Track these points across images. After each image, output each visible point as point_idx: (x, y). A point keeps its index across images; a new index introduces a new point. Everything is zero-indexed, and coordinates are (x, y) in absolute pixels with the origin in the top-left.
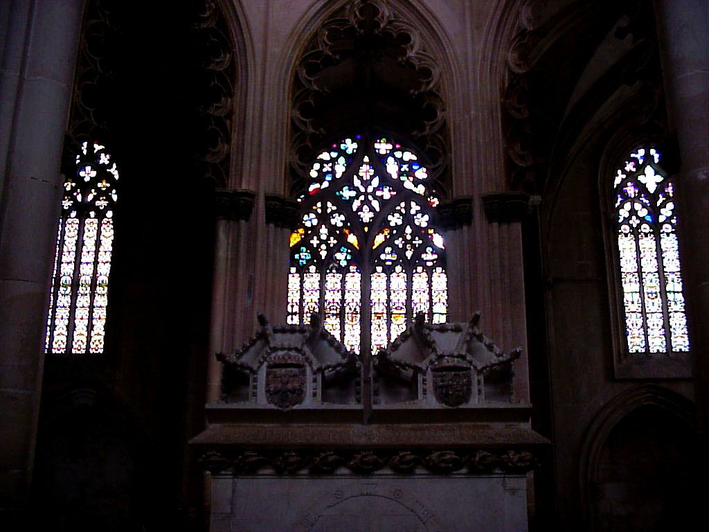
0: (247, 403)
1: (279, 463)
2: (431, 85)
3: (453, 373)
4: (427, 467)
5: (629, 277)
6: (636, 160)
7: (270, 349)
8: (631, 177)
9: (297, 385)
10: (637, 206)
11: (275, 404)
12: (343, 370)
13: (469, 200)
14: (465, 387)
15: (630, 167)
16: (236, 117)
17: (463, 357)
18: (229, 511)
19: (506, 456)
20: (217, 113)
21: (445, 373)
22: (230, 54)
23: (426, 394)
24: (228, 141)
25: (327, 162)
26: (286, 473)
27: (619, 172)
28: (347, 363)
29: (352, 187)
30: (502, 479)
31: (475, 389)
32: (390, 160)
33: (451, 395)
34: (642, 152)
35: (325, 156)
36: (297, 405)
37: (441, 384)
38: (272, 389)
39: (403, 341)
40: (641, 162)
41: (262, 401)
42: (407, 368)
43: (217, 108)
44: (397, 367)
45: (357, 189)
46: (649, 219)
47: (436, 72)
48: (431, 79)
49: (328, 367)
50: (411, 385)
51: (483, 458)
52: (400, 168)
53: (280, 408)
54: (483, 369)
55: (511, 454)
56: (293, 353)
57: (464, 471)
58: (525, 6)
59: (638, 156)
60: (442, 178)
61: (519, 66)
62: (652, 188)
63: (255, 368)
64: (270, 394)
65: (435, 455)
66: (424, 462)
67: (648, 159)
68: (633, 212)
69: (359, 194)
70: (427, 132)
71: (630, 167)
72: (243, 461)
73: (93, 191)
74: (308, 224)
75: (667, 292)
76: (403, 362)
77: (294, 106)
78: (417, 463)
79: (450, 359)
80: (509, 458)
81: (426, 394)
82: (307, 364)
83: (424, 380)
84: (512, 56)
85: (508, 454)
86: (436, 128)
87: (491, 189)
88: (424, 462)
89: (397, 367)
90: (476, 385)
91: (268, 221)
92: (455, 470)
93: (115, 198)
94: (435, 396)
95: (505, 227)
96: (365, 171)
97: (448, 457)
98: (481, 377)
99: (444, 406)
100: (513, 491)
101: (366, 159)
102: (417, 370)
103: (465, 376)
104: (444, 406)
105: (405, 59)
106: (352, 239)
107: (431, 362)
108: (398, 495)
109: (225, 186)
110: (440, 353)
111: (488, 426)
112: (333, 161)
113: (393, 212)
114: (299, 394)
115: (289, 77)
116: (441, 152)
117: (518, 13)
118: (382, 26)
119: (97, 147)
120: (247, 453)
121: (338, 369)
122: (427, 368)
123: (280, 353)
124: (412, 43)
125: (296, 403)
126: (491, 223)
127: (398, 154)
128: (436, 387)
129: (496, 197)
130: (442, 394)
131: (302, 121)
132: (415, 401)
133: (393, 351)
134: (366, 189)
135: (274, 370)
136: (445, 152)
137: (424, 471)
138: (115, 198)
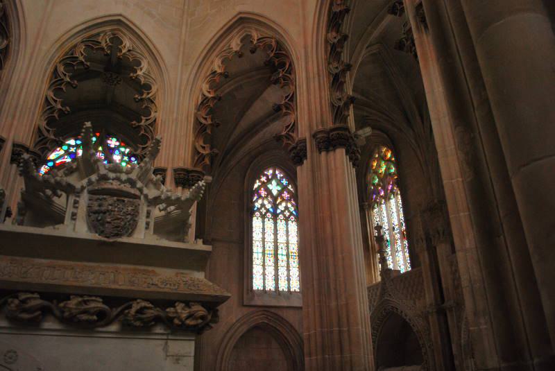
2: (150, 95)
3: (115, 198)
4: (62, 320)
5: (257, 243)
6: (267, 176)
8: (264, 185)
15: (264, 179)
17: (132, 183)
19: (172, 309)
21: (105, 196)
22: (7, 40)
23: (75, 219)
25: (73, 146)
27: (257, 181)
30: (163, 342)
32: (117, 152)
33: (108, 222)
34: (271, 172)
35: (72, 142)
37: (97, 208)
40: (270, 177)
42: (59, 192)
46: (271, 210)
52: (123, 158)
55: (180, 307)
57: (114, 328)
59: (269, 174)
61: (209, 92)
62: (275, 193)
65: (73, 303)
66: (57, 312)
67: (274, 176)
68: (263, 205)
70: (142, 123)
71: (264, 179)
77: (49, 88)
78: (46, 311)
80: (176, 312)
81: (75, 219)
83: (76, 202)
84: (205, 87)
85: (175, 307)
86: (149, 122)
87: (181, 165)
92: (103, 326)
94: (88, 223)
97: (93, 305)
99: (96, 237)
100: (177, 358)
101: (100, 149)
103: (132, 204)
104: (96, 237)
105: (135, 75)
107: (90, 183)
108: (11, 358)
111: (153, 271)
115: (50, 69)
117: (212, 62)
118: (124, 51)
122: (83, 188)
124: (142, 66)
127: (122, 149)
128: (91, 212)
130: (96, 219)
131: (54, 100)
137: (56, 326)
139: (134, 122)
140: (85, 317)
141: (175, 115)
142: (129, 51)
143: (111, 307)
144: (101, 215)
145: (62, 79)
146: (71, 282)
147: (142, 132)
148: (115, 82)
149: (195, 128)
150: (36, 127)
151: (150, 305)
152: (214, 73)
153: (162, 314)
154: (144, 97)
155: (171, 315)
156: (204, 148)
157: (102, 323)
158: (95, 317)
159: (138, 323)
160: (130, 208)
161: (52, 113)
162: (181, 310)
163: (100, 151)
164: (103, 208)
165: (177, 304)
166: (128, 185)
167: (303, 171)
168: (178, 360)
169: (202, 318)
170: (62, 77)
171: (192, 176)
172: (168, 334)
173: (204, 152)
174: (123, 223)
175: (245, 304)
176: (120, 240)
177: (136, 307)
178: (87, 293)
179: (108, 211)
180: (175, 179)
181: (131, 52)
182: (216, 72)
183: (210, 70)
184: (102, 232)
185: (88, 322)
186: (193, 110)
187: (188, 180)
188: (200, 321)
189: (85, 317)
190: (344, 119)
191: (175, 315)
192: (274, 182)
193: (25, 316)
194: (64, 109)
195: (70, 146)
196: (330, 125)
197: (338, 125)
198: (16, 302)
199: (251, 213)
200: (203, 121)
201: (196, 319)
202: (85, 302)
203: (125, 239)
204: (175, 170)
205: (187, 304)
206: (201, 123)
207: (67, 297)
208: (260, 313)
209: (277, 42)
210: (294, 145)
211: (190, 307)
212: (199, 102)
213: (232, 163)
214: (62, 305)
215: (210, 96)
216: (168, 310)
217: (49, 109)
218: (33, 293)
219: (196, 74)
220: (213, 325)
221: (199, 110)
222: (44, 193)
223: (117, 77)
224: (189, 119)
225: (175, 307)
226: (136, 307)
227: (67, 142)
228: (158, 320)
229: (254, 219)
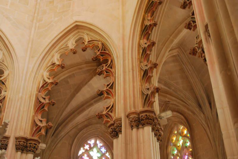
6: (90, 145)
27: (82, 148)
40: (92, 146)
47: (6, 73)
48: (3, 75)
61: (49, 79)
67: (95, 145)
71: (87, 147)
84: (46, 74)
87: (21, 134)
117: (53, 56)
126: (17, 152)
129: (23, 138)
141: (21, 94)
149: (35, 106)
152: (54, 64)
156: (41, 121)
167: (118, 143)
171: (29, 143)
173: (41, 125)
180: (16, 145)
182: (54, 64)
183: (51, 61)
186: (35, 92)
187: (26, 147)
190: (151, 104)
192: (95, 150)
196: (140, 108)
197: (146, 108)
200: (43, 101)
204: (17, 138)
206: (41, 102)
209: (103, 44)
210: (112, 122)
212: (41, 86)
213: (63, 133)
215: (49, 81)
221: (39, 92)
224: (31, 98)
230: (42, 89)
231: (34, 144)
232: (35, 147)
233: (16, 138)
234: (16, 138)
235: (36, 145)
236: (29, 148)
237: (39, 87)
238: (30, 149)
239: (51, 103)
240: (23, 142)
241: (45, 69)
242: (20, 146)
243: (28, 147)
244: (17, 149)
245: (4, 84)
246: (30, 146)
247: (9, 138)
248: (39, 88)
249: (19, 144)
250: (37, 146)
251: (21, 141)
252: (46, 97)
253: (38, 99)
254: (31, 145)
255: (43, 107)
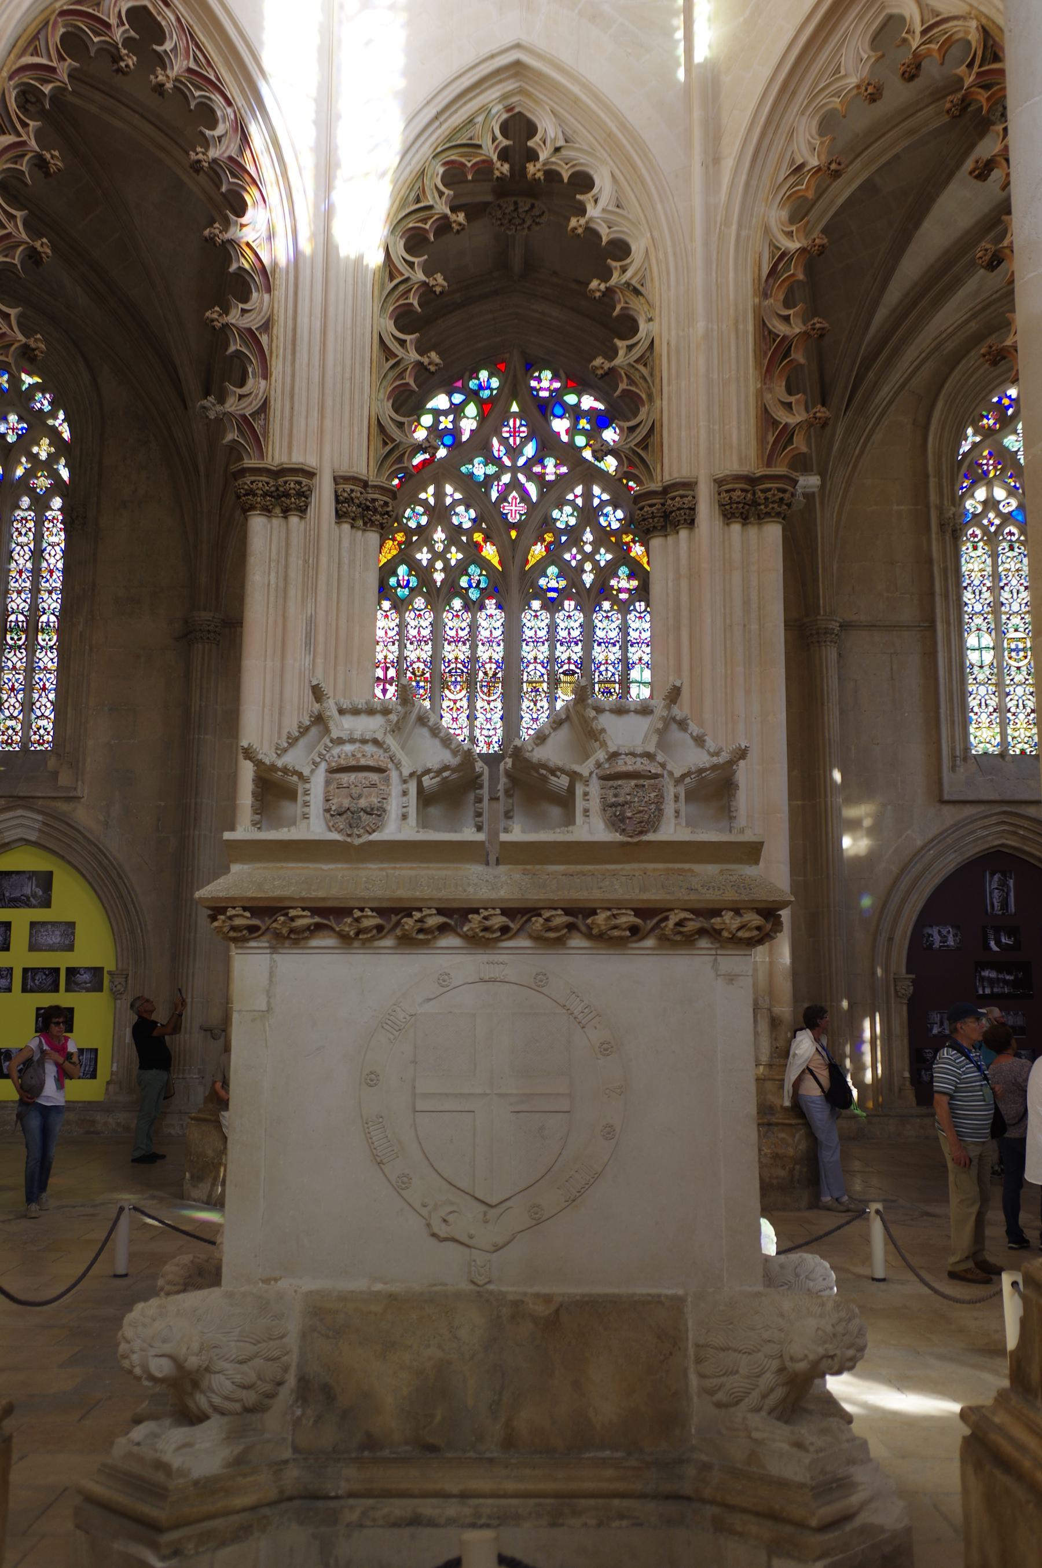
0: (293, 829)
1: (347, 929)
2: (629, 274)
3: (633, 783)
4: (589, 935)
5: (978, 620)
7: (332, 741)
9: (375, 800)
10: (999, 493)
11: (340, 831)
12: (454, 776)
13: (689, 485)
14: (653, 807)
16: (280, 330)
18: (265, 1008)
19: (719, 919)
20: (245, 322)
21: (620, 782)
24: (266, 375)
25: (446, 413)
26: (356, 944)
28: (459, 765)
29: (491, 459)
30: (712, 958)
31: (669, 808)
33: (629, 818)
35: (441, 401)
36: (375, 834)
38: (333, 808)
39: (554, 729)
41: (315, 828)
42: (558, 773)
43: (244, 311)
44: (544, 772)
45: (497, 461)
47: (637, 248)
49: (427, 772)
50: (566, 801)
51: (680, 924)
53: (349, 840)
54: (684, 776)
55: (728, 916)
56: (369, 749)
57: (650, 942)
58: (804, 119)
60: (644, 444)
61: (789, 234)
63: (306, 772)
64: (332, 816)
65: (601, 918)
66: (583, 928)
68: (990, 503)
69: (502, 469)
70: (620, 360)
72: (271, 921)
73: (24, 460)
74: (412, 524)
75: (993, 648)
76: (551, 764)
78: (571, 927)
79: (630, 760)
82: (390, 765)
83: (586, 794)
84: (777, 216)
85: (721, 916)
86: (637, 352)
87: (732, 466)
88: (583, 928)
89: (544, 772)
90: (672, 803)
91: (340, 516)
92: (636, 942)
93: (65, 474)
95: (753, 531)
96: (515, 428)
97: (623, 920)
98: (681, 790)
99: (617, 837)
101: (515, 408)
102: (574, 776)
103: (654, 788)
104: (617, 837)
105: (582, 221)
106: (490, 552)
107: (599, 765)
108: (541, 981)
109: (262, 456)
110: (612, 750)
112: (457, 410)
113: (560, 505)
114: (377, 812)
116: (644, 396)
118: (543, 157)
119: (28, 380)
120: (292, 913)
121: (445, 774)
122: (591, 773)
123: (348, 748)
124: (595, 191)
125: (374, 831)
126: (728, 524)
127: (571, 399)
128: (606, 806)
129: (738, 478)
130: (616, 815)
132: (570, 828)
133: (537, 745)
134: (514, 461)
135: (338, 776)
136: (650, 397)
137: (585, 943)
138: (65, 474)
139: (598, 361)
140: (616, 933)
142: (557, 150)
143: (644, 919)
144: (619, 808)
145: (407, 279)
146: (597, 894)
147: (622, 386)
148: (528, 223)
150: (373, 413)
151: (692, 916)
153: (706, 925)
154: (613, 282)
155: (717, 927)
156: (788, 406)
157: (634, 938)
158: (628, 933)
159: (678, 938)
160: (653, 795)
161: (401, 376)
162: (729, 921)
163: (515, 415)
164: (621, 800)
165: (723, 913)
166: (645, 761)
168: (732, 980)
169: (758, 928)
170: (406, 272)
171: (764, 491)
172: (717, 949)
174: (646, 816)
175: (946, 797)
176: (645, 838)
177: (673, 919)
178: (614, 907)
179: (626, 803)
180: (721, 505)
181: (564, 152)
184: (624, 830)
185: (621, 938)
186: (749, 301)
187: (755, 503)
188: (755, 933)
189: (616, 933)
191: (723, 926)
193: (552, 935)
194: (425, 360)
195: (437, 413)
198: (541, 920)
199: (954, 530)
200: (781, 328)
201: (750, 929)
202: (614, 916)
203: (650, 837)
204: (719, 482)
205: (737, 912)
207: (593, 912)
208: (994, 820)
209: (985, 31)
211: (741, 916)
212: (765, 271)
213: (885, 391)
214: (589, 921)
216: (713, 921)
217: (392, 367)
218: (555, 909)
219: (747, 184)
220: (772, 934)
221: (765, 295)
222: (538, 772)
223: (533, 206)
225: (721, 916)
226: (673, 919)
227: (429, 406)
228: (702, 932)
229: (966, 548)
230: (771, 281)
231: (779, 490)
232: (782, 499)
233: (715, 480)
234: (715, 480)
235: (784, 491)
236: (762, 507)
237: (759, 276)
238: (768, 510)
239: (812, 333)
240: (743, 490)
241: (771, 197)
242: (734, 506)
243: (760, 505)
244: (724, 515)
245: (642, 294)
246: (766, 499)
247: (696, 483)
248: (759, 280)
249: (730, 498)
250: (787, 495)
251: (734, 490)
252: (791, 312)
253: (764, 324)
254: (769, 494)
255: (787, 354)
